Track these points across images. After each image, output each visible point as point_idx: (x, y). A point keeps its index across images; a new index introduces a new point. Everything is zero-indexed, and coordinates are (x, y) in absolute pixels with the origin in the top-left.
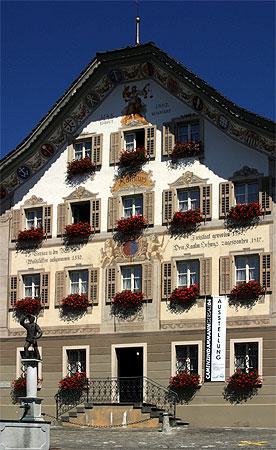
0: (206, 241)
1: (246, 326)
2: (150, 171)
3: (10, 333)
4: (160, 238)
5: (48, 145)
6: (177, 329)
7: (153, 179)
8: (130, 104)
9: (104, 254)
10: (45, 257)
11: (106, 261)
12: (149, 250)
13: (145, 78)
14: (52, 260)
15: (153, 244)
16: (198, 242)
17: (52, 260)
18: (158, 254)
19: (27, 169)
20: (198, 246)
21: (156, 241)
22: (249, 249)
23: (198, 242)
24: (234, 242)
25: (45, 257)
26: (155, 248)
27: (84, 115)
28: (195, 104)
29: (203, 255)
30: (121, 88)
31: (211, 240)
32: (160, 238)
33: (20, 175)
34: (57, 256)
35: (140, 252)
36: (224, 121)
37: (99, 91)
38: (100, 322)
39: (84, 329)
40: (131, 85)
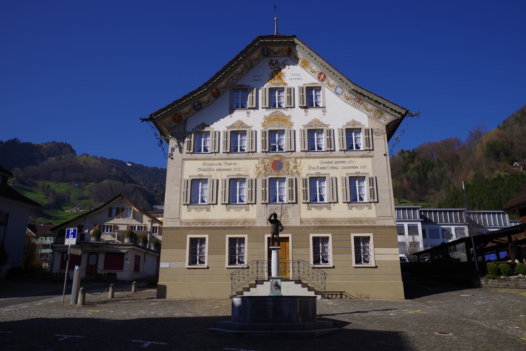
0: (330, 165)
1: (361, 225)
2: (290, 116)
3: (181, 222)
4: (298, 161)
5: (217, 90)
6: (313, 225)
7: (292, 120)
8: (274, 71)
9: (258, 168)
10: (212, 167)
11: (260, 173)
12: (291, 168)
13: (285, 56)
14: (217, 170)
15: (294, 164)
16: (325, 165)
17: (217, 170)
18: (297, 171)
19: (200, 104)
20: (325, 168)
21: (295, 162)
22: (359, 173)
23: (325, 165)
24: (349, 168)
25: (212, 167)
26: (295, 167)
27: (242, 73)
28: (319, 78)
29: (328, 174)
30: (268, 60)
31: (334, 165)
32: (298, 161)
33: (194, 107)
34: (222, 167)
35: (284, 169)
36: (339, 90)
37: (254, 60)
38: (256, 218)
39: (243, 222)
40: (275, 59)
